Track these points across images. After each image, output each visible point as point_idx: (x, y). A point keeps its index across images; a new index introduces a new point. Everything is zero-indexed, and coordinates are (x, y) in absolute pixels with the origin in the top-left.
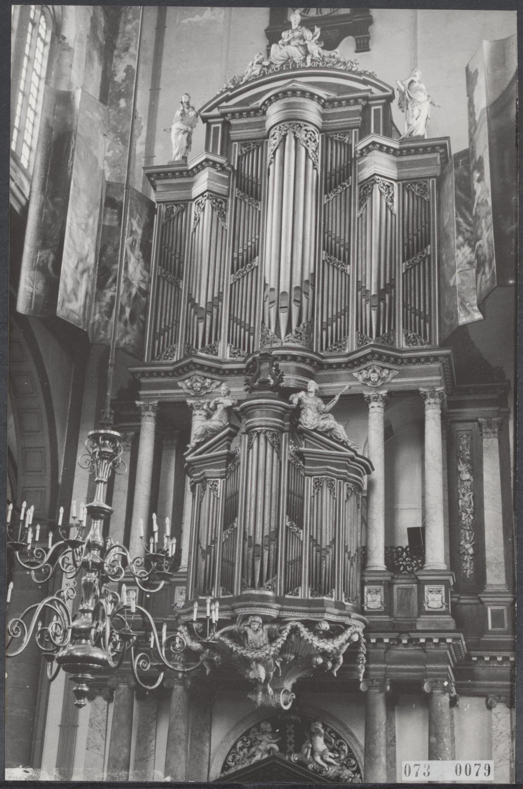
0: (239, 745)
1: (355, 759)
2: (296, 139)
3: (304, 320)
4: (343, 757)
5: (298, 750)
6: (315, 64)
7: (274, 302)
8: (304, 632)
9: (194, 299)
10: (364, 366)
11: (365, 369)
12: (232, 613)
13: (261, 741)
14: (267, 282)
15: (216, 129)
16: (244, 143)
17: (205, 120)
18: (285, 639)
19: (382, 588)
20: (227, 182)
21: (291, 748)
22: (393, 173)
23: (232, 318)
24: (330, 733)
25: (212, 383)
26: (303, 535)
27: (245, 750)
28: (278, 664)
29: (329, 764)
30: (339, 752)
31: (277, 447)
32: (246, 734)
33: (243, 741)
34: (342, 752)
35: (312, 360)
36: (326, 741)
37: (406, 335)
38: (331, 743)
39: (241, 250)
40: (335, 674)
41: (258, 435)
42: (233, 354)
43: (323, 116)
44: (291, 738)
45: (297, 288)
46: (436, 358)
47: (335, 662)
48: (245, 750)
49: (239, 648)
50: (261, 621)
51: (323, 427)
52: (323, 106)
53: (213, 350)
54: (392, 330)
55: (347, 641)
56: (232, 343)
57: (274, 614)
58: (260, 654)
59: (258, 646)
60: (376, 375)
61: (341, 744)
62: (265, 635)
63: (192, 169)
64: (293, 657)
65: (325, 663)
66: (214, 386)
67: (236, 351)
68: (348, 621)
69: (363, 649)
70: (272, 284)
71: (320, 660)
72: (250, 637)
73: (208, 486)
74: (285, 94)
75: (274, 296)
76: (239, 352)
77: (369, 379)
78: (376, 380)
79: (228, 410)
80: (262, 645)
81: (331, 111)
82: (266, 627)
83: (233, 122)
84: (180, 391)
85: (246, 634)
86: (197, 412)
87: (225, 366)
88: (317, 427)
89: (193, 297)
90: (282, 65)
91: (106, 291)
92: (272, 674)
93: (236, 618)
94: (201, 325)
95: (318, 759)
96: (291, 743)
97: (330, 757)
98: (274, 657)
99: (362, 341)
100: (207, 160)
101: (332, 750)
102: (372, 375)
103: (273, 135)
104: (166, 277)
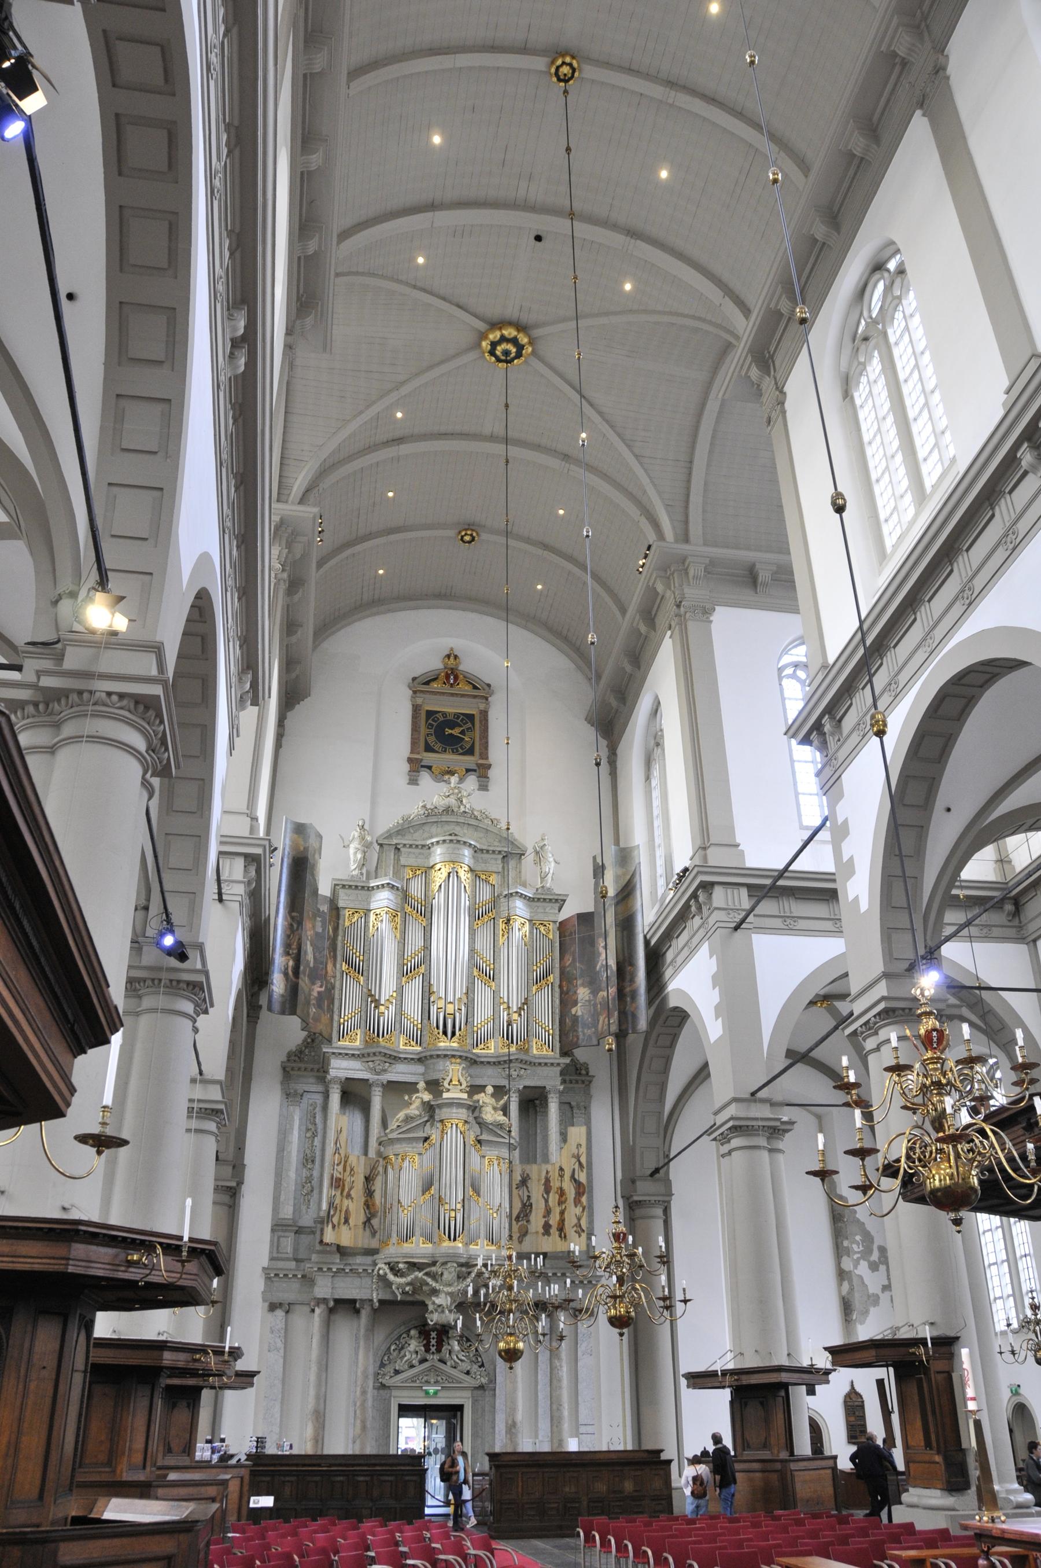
0: (393, 1348)
2: (457, 876)
9: (375, 996)
12: (433, 1259)
17: (381, 845)
21: (433, 1349)
27: (397, 1351)
29: (462, 1361)
32: (399, 1338)
35: (471, 1059)
44: (433, 1342)
45: (460, 999)
46: (558, 1064)
48: (397, 1351)
52: (475, 852)
58: (449, 1289)
60: (516, 1073)
63: (373, 887)
66: (389, 1069)
74: (451, 841)
82: (459, 1269)
85: (442, 1274)
86: (378, 1089)
89: (373, 993)
96: (433, 1346)
100: (388, 884)
102: (514, 1073)
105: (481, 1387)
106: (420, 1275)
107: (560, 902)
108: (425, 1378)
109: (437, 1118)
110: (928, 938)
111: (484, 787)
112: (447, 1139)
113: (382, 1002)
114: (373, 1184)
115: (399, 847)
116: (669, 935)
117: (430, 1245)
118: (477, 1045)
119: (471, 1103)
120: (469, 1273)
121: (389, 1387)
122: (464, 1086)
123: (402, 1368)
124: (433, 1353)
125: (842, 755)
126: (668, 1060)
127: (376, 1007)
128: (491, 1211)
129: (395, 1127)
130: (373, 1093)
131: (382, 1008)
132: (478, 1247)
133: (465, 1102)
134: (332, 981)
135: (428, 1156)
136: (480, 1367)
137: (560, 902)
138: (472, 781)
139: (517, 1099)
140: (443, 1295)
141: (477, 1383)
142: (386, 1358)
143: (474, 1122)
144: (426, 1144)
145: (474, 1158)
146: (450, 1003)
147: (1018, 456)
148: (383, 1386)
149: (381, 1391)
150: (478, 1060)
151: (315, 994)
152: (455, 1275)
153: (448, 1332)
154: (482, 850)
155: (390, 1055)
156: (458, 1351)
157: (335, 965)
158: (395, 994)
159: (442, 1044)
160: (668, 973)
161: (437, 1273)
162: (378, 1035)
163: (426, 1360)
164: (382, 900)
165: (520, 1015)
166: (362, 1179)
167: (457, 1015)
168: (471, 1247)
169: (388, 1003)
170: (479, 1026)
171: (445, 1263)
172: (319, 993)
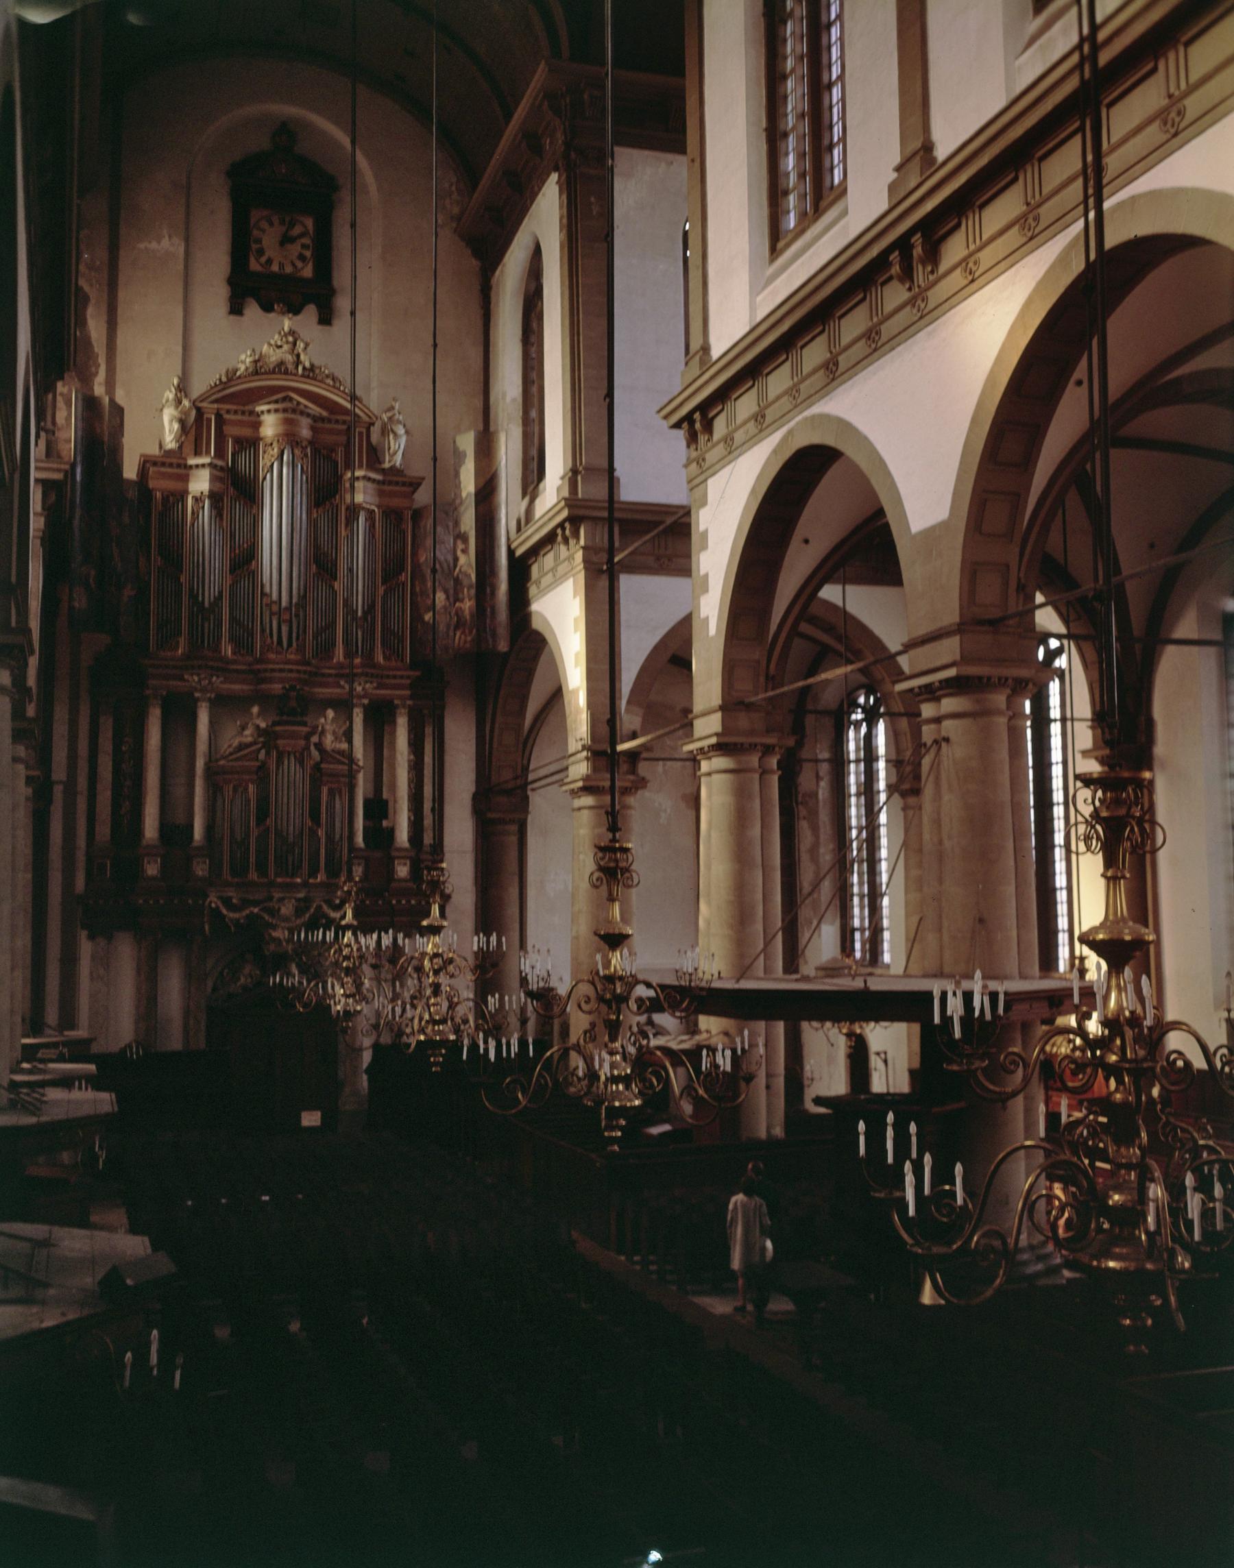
6: (307, 373)
8: (325, 907)
14: (267, 590)
15: (209, 420)
16: (238, 441)
17: (199, 410)
19: (363, 862)
20: (221, 479)
22: (376, 500)
23: (233, 619)
26: (321, 833)
31: (301, 762)
37: (384, 653)
39: (237, 551)
41: (289, 754)
42: (234, 653)
43: (313, 428)
46: (408, 677)
52: (315, 421)
53: (217, 649)
54: (372, 650)
57: (301, 895)
70: (275, 596)
73: (240, 790)
74: (285, 410)
75: (275, 608)
81: (320, 425)
83: (227, 416)
84: (187, 684)
85: (279, 909)
86: (204, 704)
90: (274, 368)
99: (349, 654)
103: (271, 444)
106: (256, 910)
107: (415, 484)
110: (772, 666)
111: (326, 319)
113: (207, 604)
115: (222, 412)
116: (535, 551)
120: (308, 908)
125: (711, 457)
126: (530, 674)
137: (415, 484)
138: (311, 312)
143: (312, 748)
147: (891, 258)
154: (322, 419)
157: (149, 560)
160: (533, 590)
162: (203, 642)
164: (200, 484)
165: (367, 620)
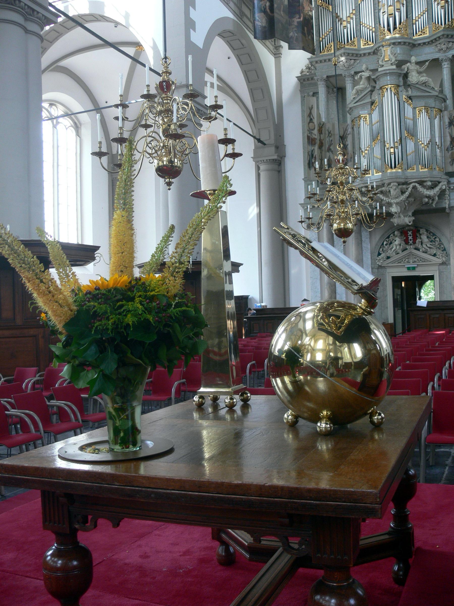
0: (385, 243)
1: (443, 244)
3: (402, 21)
4: (437, 244)
5: (414, 243)
7: (385, 12)
10: (439, 42)
11: (440, 44)
12: (382, 182)
13: (395, 241)
18: (410, 192)
21: (411, 242)
24: (429, 233)
25: (355, 62)
27: (388, 245)
28: (406, 204)
29: (430, 248)
30: (434, 241)
33: (387, 241)
34: (436, 242)
35: (409, 43)
36: (428, 237)
38: (430, 238)
40: (434, 206)
41: (387, 89)
44: (410, 238)
47: (433, 200)
49: (387, 199)
50: (397, 185)
51: (422, 82)
55: (440, 189)
56: (363, 38)
59: (396, 197)
61: (435, 238)
62: (400, 191)
64: (413, 200)
65: (428, 201)
66: (356, 64)
67: (366, 42)
68: (440, 180)
69: (447, 192)
71: (426, 200)
72: (392, 193)
76: (368, 43)
77: (442, 49)
78: (446, 49)
79: (369, 78)
80: (398, 196)
82: (400, 187)
85: (390, 191)
87: (361, 52)
88: (418, 82)
91: (293, 19)
92: (403, 209)
93: (384, 184)
94: (345, 30)
95: (424, 246)
96: (411, 240)
97: (431, 245)
98: (404, 201)
101: (431, 241)
104: (323, 5)
105: (443, 263)
108: (407, 260)
109: (378, 87)
112: (385, 100)
113: (345, 19)
114: (346, 140)
117: (381, 174)
118: (416, 33)
119: (399, 72)
121: (384, 267)
122: (393, 60)
123: (391, 255)
124: (411, 244)
127: (341, 24)
128: (423, 145)
129: (352, 98)
130: (347, 82)
131: (345, 24)
132: (415, 171)
133: (395, 71)
134: (310, 13)
135: (375, 116)
136: (443, 251)
139: (449, 66)
140: (394, 206)
141: (440, 261)
142: (381, 250)
144: (372, 107)
145: (409, 111)
146: (390, 6)
148: (380, 267)
149: (380, 270)
150: (416, 43)
151: (296, 24)
152: (398, 190)
153: (419, 231)
155: (353, 54)
156: (427, 242)
158: (354, 12)
159: (388, 37)
161: (386, 191)
163: (407, 249)
166: (337, 137)
167: (397, 14)
168: (408, 171)
169: (349, 19)
170: (417, 19)
171: (389, 184)
172: (298, 22)
